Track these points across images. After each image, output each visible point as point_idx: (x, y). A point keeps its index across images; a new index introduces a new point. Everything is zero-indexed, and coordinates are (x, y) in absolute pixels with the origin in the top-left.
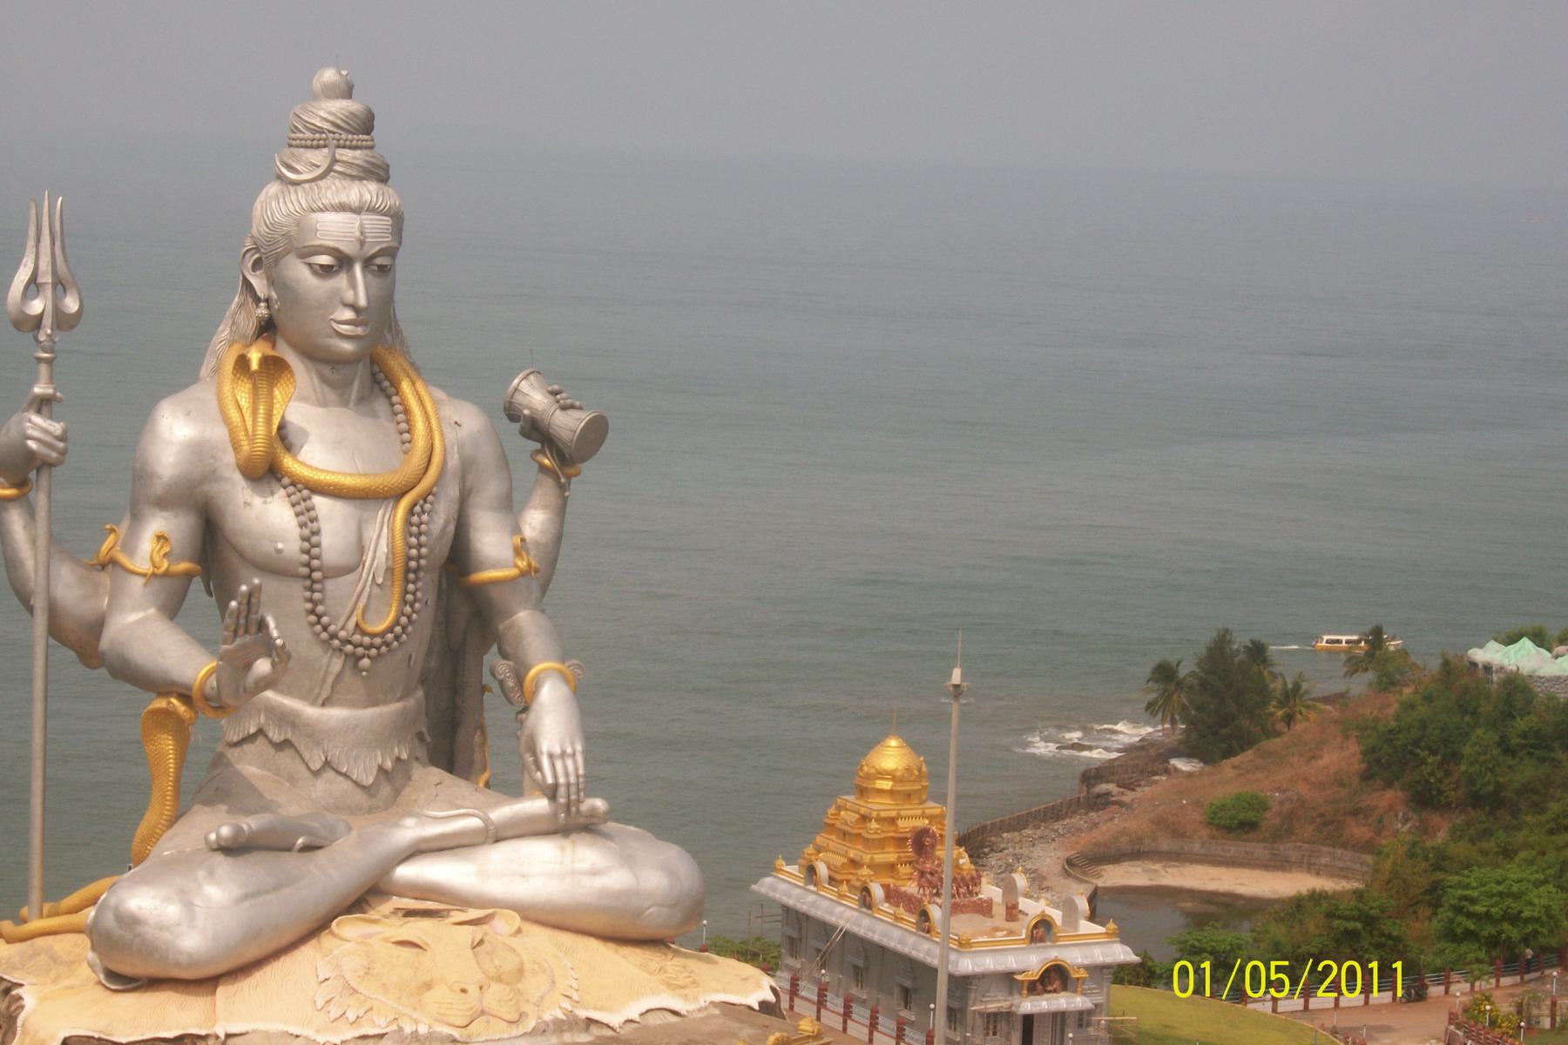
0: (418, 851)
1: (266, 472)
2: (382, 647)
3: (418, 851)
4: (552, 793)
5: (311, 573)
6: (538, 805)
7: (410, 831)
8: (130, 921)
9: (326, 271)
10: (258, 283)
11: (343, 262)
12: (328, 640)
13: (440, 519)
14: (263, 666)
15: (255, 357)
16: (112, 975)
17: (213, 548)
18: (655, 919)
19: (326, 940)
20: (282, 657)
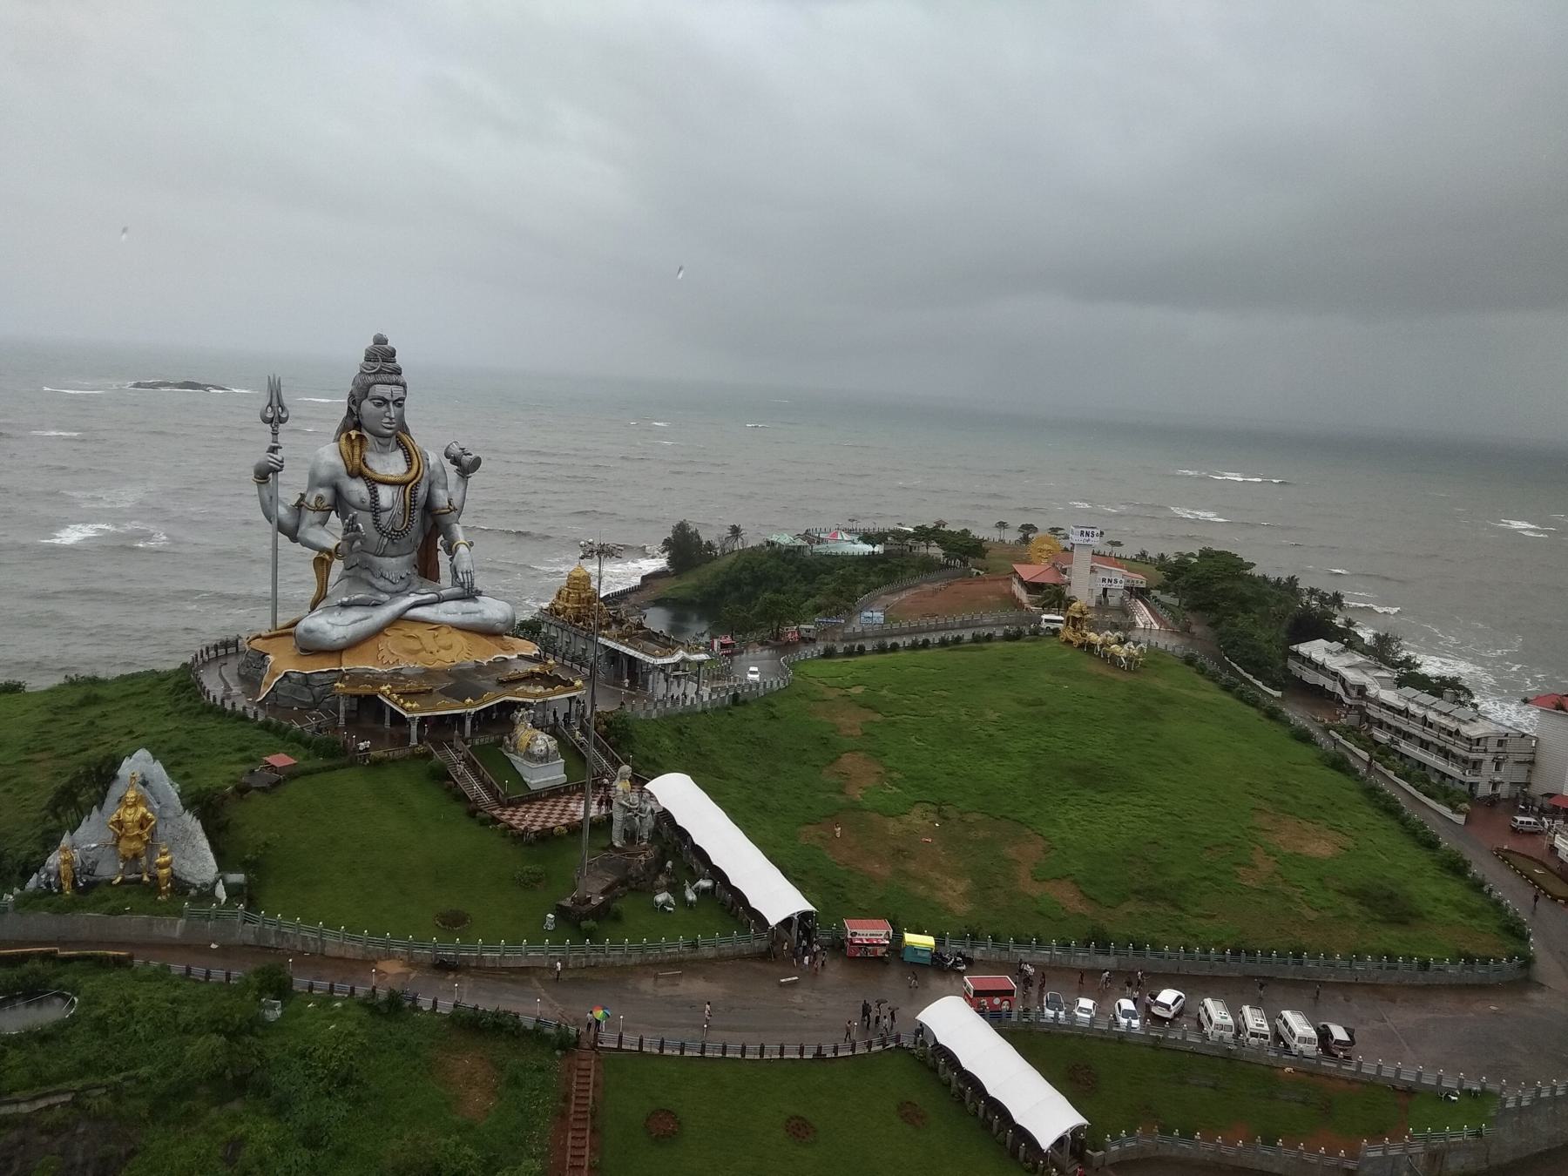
0: (416, 605)
1: (356, 473)
2: (401, 534)
3: (416, 605)
4: (462, 585)
5: (375, 508)
6: (457, 590)
7: (413, 599)
8: (309, 631)
9: (379, 405)
10: (354, 408)
11: (386, 402)
12: (382, 533)
13: (422, 491)
14: (358, 543)
15: (353, 433)
16: (303, 650)
17: (339, 502)
18: (500, 627)
19: (382, 637)
20: (364, 540)
